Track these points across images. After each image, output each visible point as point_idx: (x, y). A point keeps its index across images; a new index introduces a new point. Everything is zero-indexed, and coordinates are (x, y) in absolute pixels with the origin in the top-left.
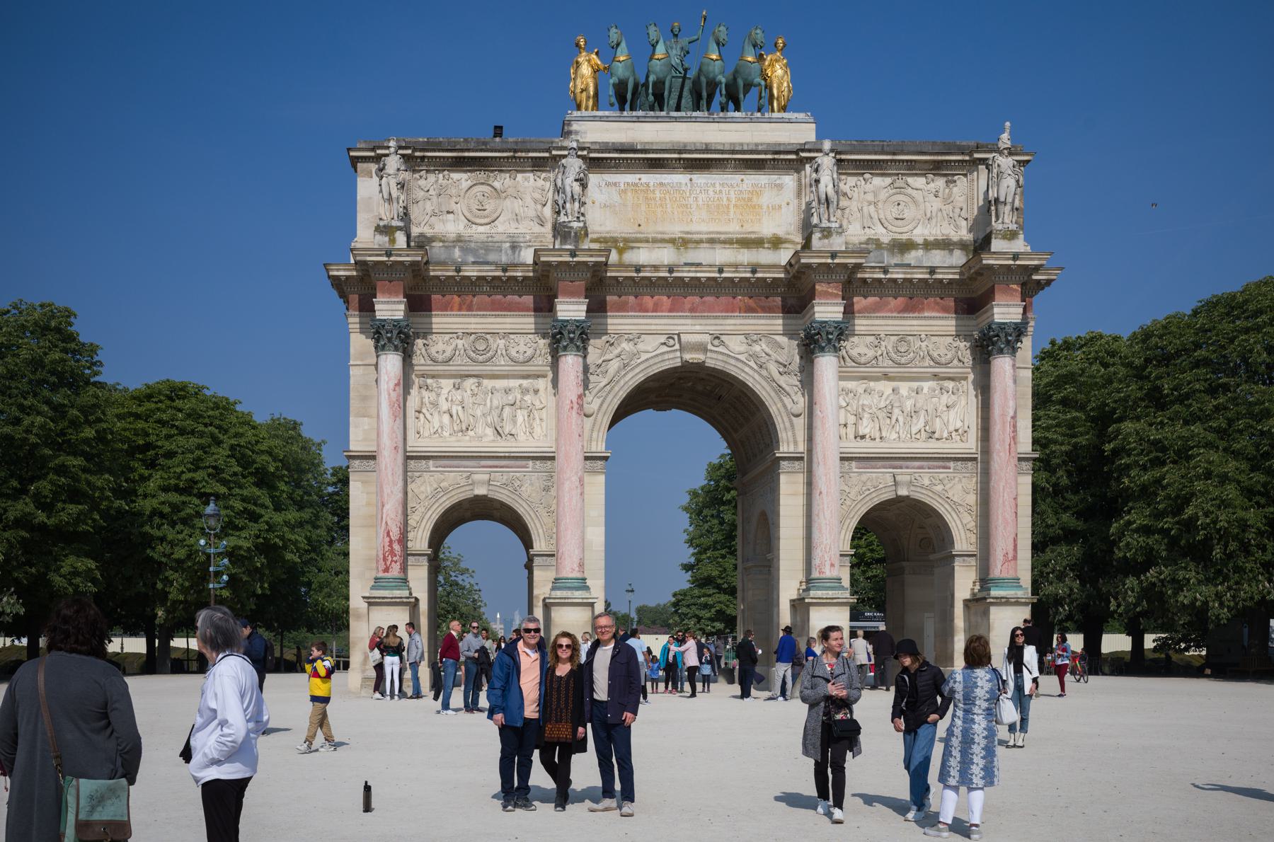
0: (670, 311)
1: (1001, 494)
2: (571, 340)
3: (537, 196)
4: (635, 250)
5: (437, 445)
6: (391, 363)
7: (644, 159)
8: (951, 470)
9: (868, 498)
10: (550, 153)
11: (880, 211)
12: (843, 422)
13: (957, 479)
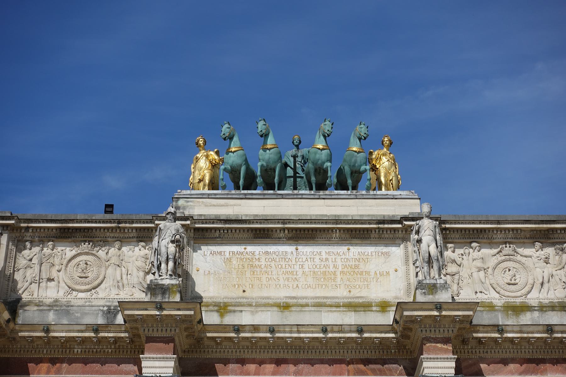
4: (238, 314)
7: (249, 229)
10: (154, 223)
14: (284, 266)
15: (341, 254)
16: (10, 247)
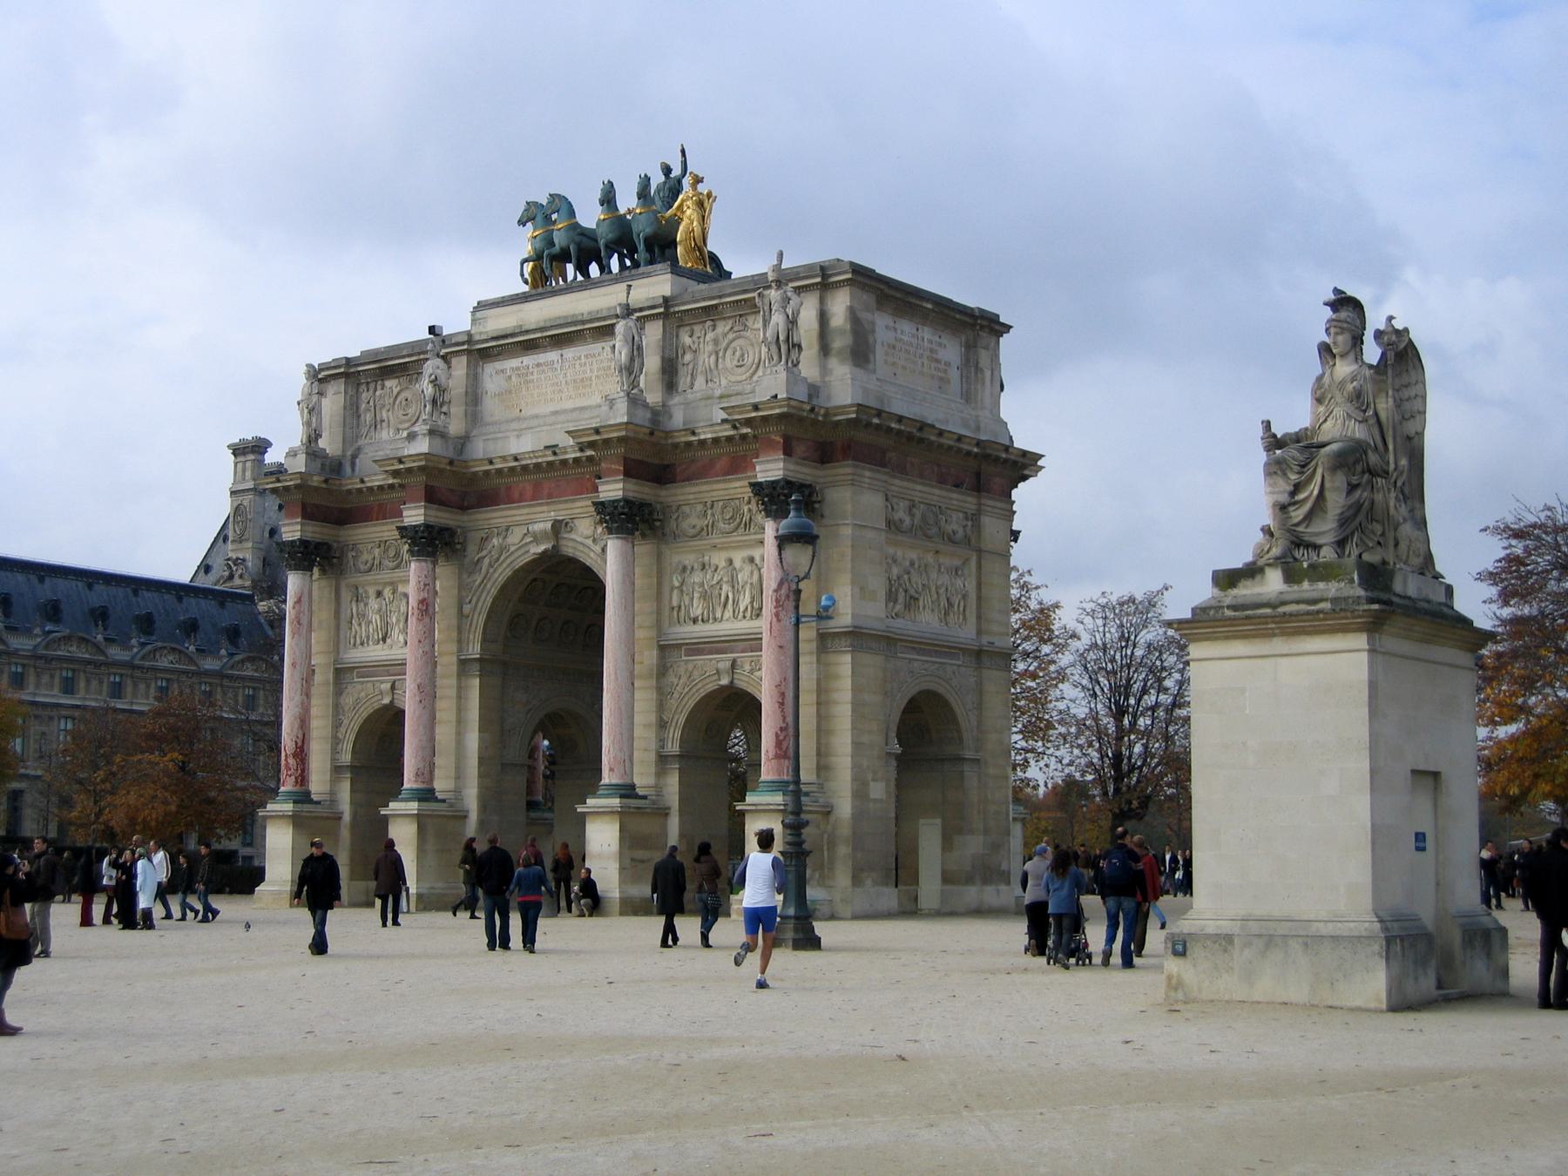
5: (358, 655)
7: (517, 342)
9: (694, 690)
11: (720, 360)
12: (675, 603)
16: (350, 393)
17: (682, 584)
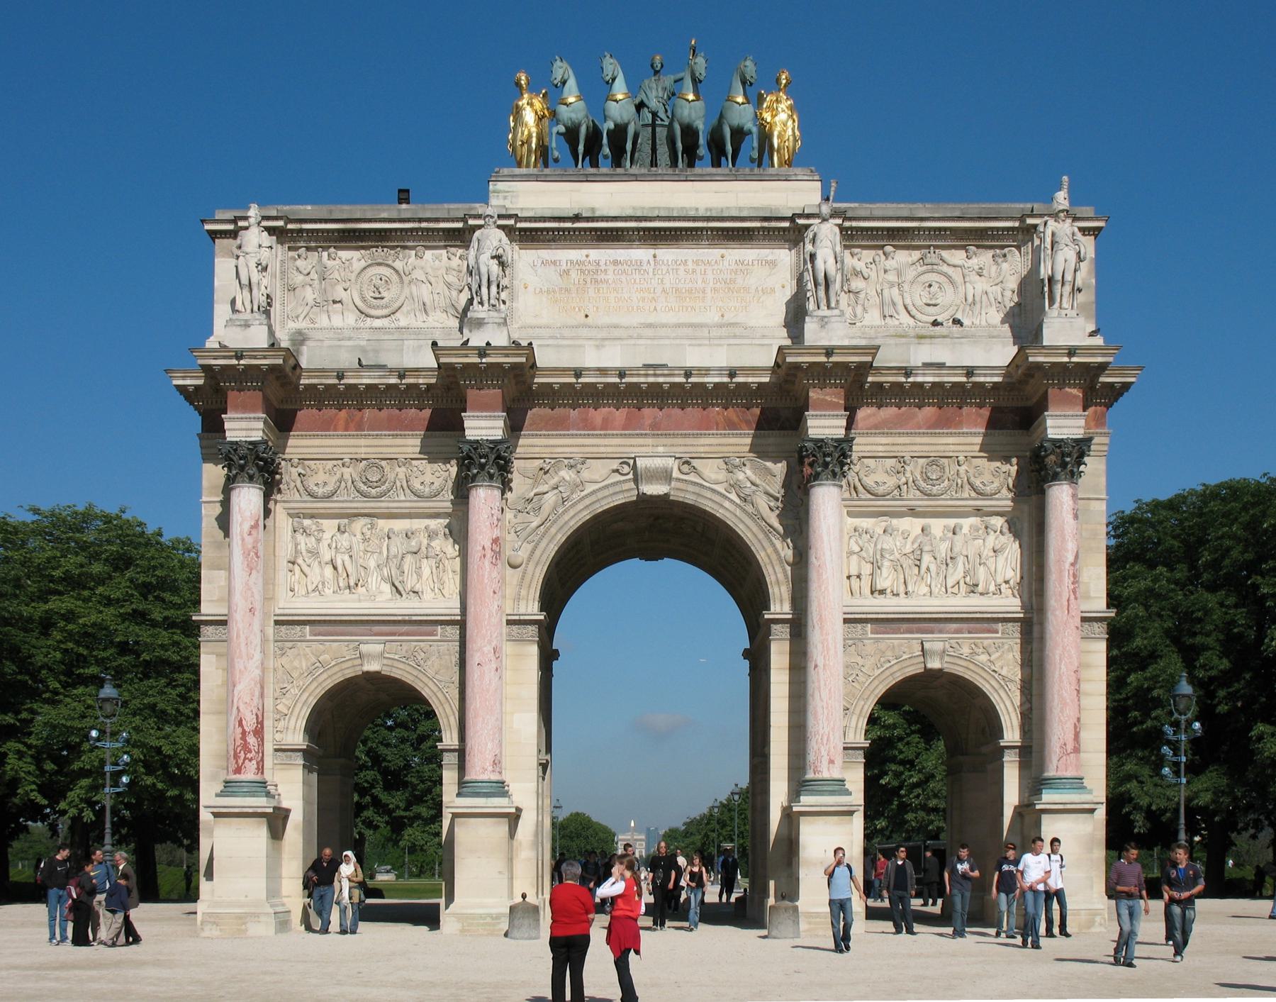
0: (623, 429)
1: (1058, 666)
2: (482, 467)
3: (451, 278)
6: (248, 498)
7: (591, 229)
8: (999, 635)
9: (888, 673)
12: (854, 572)
13: (1006, 647)
14: (638, 281)
15: (713, 263)
17: (862, 550)
